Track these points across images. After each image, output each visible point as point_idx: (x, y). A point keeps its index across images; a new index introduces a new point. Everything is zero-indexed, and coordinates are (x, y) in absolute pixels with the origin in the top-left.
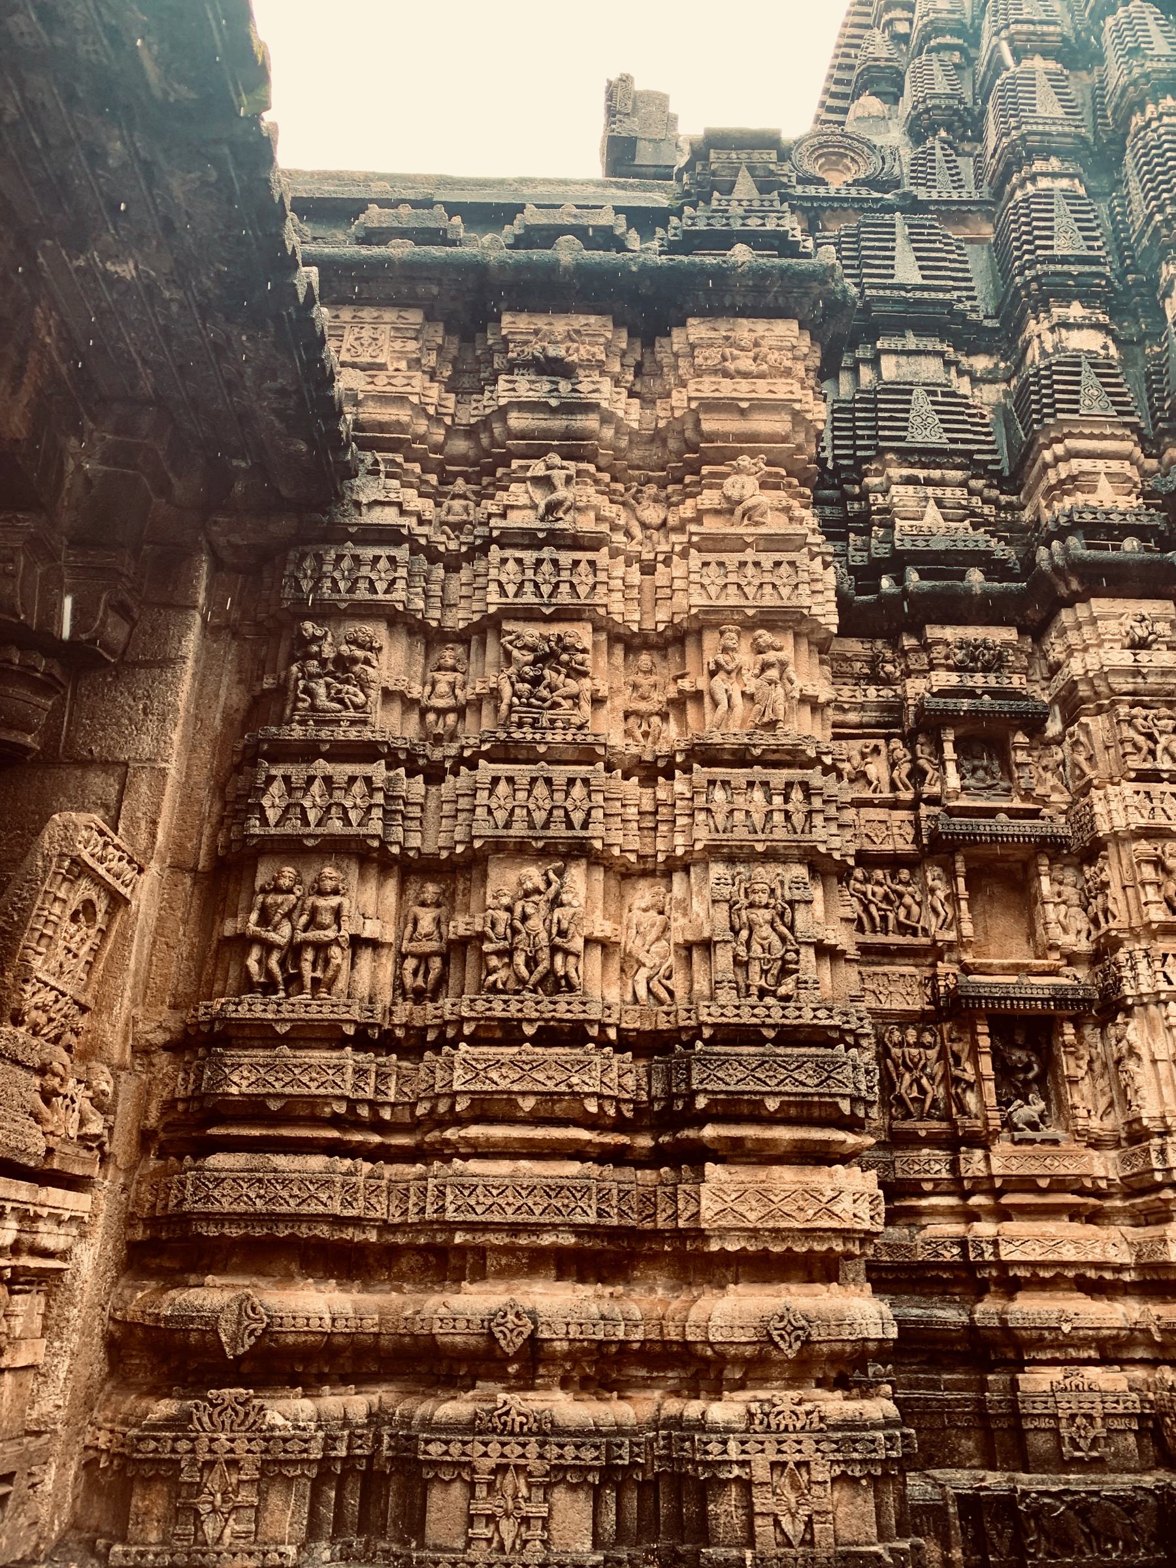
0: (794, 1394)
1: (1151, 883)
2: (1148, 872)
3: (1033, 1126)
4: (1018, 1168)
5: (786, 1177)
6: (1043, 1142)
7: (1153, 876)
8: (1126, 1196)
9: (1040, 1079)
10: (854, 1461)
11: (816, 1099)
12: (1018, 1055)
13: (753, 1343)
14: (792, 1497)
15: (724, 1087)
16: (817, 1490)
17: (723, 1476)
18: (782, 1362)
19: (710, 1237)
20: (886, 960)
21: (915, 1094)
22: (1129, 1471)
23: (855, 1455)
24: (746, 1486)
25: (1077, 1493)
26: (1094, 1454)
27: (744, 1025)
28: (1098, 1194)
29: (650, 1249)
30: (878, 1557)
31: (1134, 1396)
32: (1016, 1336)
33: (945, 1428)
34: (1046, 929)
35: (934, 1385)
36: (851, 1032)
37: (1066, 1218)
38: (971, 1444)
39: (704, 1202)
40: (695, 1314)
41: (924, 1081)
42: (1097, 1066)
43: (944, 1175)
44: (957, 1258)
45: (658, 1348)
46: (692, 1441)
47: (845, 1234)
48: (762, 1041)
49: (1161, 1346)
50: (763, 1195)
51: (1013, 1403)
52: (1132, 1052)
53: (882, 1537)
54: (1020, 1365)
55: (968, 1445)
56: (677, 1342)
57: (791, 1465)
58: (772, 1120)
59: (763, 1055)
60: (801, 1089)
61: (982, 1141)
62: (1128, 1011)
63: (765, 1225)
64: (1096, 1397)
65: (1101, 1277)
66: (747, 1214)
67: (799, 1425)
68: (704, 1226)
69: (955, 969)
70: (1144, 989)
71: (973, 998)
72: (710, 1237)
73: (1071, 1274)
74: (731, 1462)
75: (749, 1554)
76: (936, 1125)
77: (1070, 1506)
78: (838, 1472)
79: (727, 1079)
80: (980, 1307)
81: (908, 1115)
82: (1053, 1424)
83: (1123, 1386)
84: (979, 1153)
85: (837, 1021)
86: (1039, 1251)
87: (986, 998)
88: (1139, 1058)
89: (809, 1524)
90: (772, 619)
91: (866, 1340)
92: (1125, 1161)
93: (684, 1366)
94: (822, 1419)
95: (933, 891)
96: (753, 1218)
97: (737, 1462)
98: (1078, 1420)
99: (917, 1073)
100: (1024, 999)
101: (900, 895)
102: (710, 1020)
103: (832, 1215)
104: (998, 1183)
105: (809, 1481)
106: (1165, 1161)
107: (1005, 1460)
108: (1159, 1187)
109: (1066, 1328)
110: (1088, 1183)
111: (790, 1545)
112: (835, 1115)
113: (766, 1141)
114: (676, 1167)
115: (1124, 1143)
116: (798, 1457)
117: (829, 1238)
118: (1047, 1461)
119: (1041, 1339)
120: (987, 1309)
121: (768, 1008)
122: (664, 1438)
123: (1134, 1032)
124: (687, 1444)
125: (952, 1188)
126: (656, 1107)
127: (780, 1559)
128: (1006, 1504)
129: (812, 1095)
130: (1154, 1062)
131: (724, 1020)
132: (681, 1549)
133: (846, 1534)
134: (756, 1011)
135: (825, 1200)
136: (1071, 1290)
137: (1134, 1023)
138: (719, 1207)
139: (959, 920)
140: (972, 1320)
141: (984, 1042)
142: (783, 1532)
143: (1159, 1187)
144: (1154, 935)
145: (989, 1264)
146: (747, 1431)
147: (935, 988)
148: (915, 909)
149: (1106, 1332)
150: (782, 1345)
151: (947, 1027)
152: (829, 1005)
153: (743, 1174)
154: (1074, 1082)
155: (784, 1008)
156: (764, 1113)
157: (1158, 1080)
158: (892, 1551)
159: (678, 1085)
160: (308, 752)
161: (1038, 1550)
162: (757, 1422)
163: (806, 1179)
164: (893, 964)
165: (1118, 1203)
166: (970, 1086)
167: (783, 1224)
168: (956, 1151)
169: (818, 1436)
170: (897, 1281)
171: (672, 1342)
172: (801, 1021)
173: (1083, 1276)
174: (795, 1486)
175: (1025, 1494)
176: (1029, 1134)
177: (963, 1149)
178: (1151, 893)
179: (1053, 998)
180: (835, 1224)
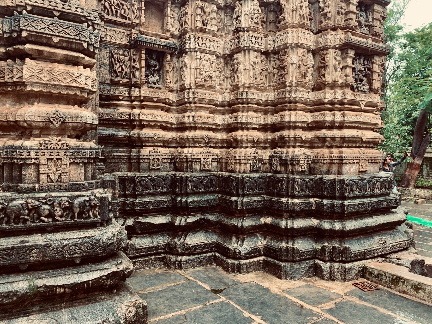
0: (58, 139)
1: (199, 15)
2: (199, 11)
3: (155, 83)
4: (148, 95)
5: (61, 68)
6: (157, 88)
7: (200, 12)
8: (177, 106)
9: (158, 70)
10: (78, 158)
11: (74, 41)
12: (153, 62)
13: (43, 122)
14: (55, 169)
15: (35, 30)
16: (63, 166)
17: (28, 162)
18: (54, 129)
19: (26, 85)
20: (115, 26)
21: (120, 70)
22: (166, 171)
23: (78, 156)
24: (37, 166)
25: (151, 176)
26: (158, 168)
27: (45, 8)
28: (170, 105)
29: (4, 90)
30: (84, 184)
31: (170, 154)
32: (141, 139)
33: (118, 162)
34: (167, 25)
35: (117, 152)
36: (91, 20)
37: (160, 110)
38: (125, 166)
39: (24, 72)
40: (20, 112)
41: (123, 67)
42: (175, 69)
43: (126, 95)
44: (128, 119)
45: (5, 124)
46: (16, 152)
47: (82, 89)
48: (53, 16)
49: (179, 143)
50: (50, 72)
51: (138, 156)
52: (185, 65)
53: (85, 179)
54: (142, 147)
55: (124, 166)
56: (13, 121)
57: (55, 159)
58: (55, 46)
59: (53, 21)
60: (68, 36)
61: (138, 86)
62: (186, 53)
63: (50, 83)
64: (161, 154)
65: (167, 126)
66: (43, 78)
67: (58, 147)
68: (25, 80)
69: (137, 32)
70: (192, 47)
71: (142, 41)
72: (26, 85)
73: (159, 124)
74: (32, 158)
75: (37, 185)
76: (125, 80)
77: (149, 179)
78: (72, 161)
79: (37, 27)
80: (132, 132)
81: (117, 76)
82: (148, 161)
83: (168, 152)
84: (137, 90)
85: (85, 14)
86: (151, 117)
87: (146, 42)
88: (187, 67)
89: (60, 176)
91: (86, 123)
92: (178, 96)
93: (17, 130)
94: (67, 146)
95: (133, 5)
96: (45, 80)
97: (34, 158)
98: (155, 160)
99: (121, 64)
100: (157, 45)
101: (123, 5)
102: (30, 3)
103: (77, 82)
104: (142, 98)
105: (61, 164)
106: (189, 96)
107: (134, 170)
108: (186, 103)
109: (155, 137)
110: (167, 101)
111: (53, 182)
112: (81, 49)
113: (53, 53)
114: (14, 60)
115: (179, 92)
116: (57, 157)
117: (75, 90)
118: (145, 170)
119: (148, 140)
120: (135, 133)
121: (57, 4)
122: (6, 152)
123: (187, 59)
124: (15, 153)
125: (128, 99)
126: (6, 36)
127: (49, 186)
128: (133, 180)
129: (73, 39)
130: (191, 68)
131: (37, 4)
132: (11, 185)
133: (73, 179)
134: (51, 3)
135: (75, 77)
136: (158, 128)
137: (187, 57)
138: (31, 74)
139: (141, 16)
140: (130, 135)
141: (143, 56)
142: (50, 179)
143: (186, 103)
144: (197, 31)
145: (136, 121)
146: (39, 149)
147: (130, 38)
148: (127, 11)
149: (166, 139)
150: (54, 122)
151: (132, 50)
152: (82, 7)
153: (43, 65)
154: (168, 72)
155: (63, 5)
156: (53, 43)
157: (191, 74)
158: (88, 183)
159: (14, 27)
161: (139, 190)
162: (42, 146)
163: (68, 69)
164: (118, 28)
165: (175, 108)
166: (137, 69)
167: (57, 83)
168: (131, 88)
169: (66, 151)
170: (109, 124)
171: (10, 121)
172: (70, 11)
173: (162, 125)
174: (56, 165)
175: (138, 177)
176: (153, 85)
177: (133, 88)
178: (199, 18)
179: (166, 46)
180: (78, 85)
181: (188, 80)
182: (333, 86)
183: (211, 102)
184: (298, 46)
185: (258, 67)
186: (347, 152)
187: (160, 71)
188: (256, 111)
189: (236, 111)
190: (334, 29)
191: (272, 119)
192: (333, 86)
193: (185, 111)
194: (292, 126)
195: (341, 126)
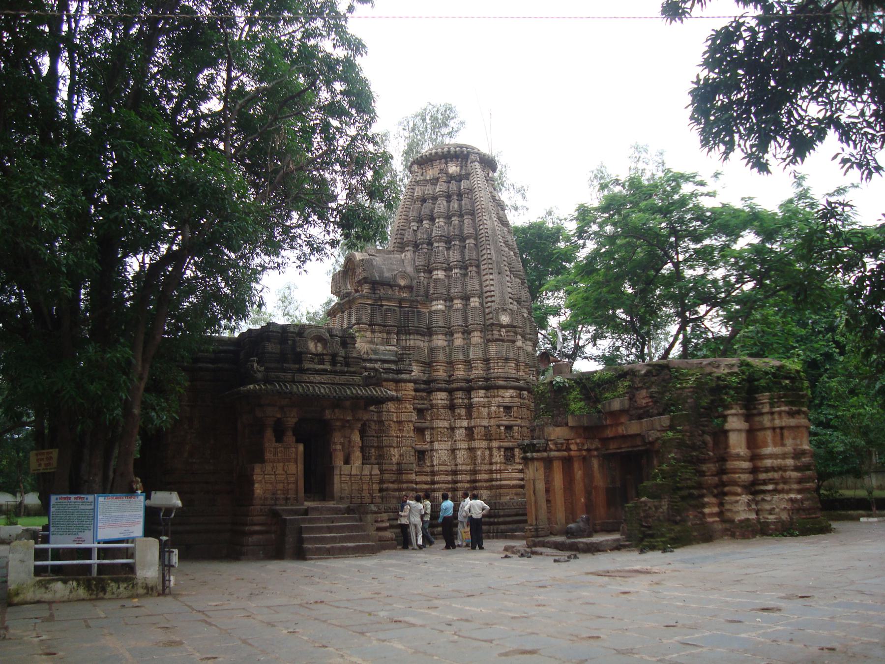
90: (409, 421)
160: (368, 436)
181: (435, 463)
182: (496, 463)
183: (446, 471)
184: (480, 448)
185: (465, 456)
186: (502, 491)
187: (424, 460)
188: (466, 474)
189: (457, 475)
190: (495, 440)
191: (473, 477)
192: (496, 463)
193: (434, 475)
194: (479, 481)
195: (501, 480)
